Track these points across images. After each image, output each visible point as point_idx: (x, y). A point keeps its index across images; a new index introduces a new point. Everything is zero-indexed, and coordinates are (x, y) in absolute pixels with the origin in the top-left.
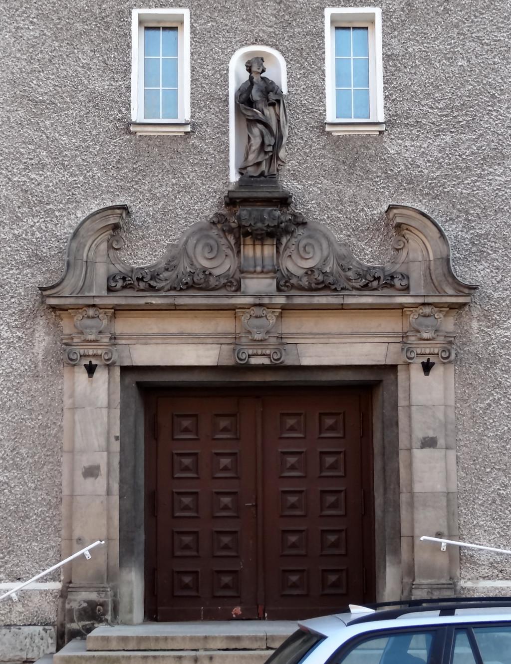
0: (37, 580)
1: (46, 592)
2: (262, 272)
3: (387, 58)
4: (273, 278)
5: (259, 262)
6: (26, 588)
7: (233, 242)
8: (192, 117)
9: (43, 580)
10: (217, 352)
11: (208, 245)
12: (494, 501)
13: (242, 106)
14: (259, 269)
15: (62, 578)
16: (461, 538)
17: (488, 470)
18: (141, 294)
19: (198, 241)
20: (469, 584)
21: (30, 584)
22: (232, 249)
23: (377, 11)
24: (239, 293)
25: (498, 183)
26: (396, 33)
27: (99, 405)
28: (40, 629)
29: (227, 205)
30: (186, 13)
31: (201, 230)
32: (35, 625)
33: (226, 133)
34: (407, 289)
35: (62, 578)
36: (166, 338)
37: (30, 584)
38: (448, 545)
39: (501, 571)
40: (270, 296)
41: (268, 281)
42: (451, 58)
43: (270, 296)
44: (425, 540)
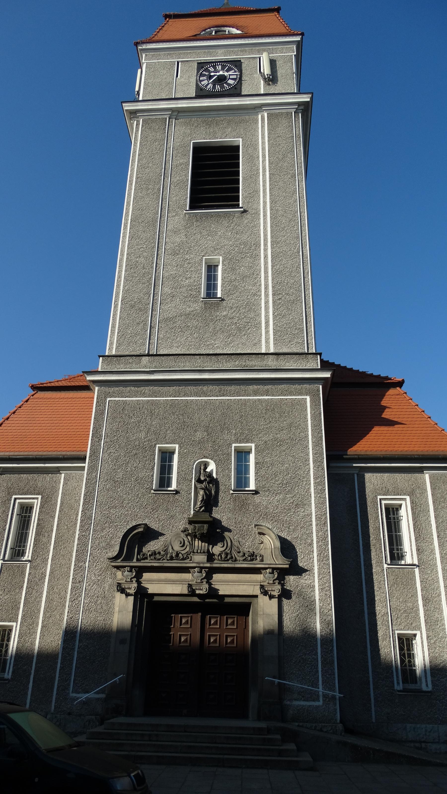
0: (95, 693)
1: (98, 699)
2: (201, 553)
3: (256, 464)
4: (205, 555)
5: (200, 548)
6: (89, 697)
7: (190, 540)
8: (177, 487)
9: (97, 693)
10: (181, 588)
11: (179, 540)
12: (300, 662)
13: (196, 483)
14: (199, 551)
15: (106, 692)
16: (284, 680)
17: (297, 646)
18: (151, 561)
19: (176, 539)
20: (288, 703)
21: (91, 695)
22: (189, 542)
23: (253, 445)
24: (191, 562)
25: (301, 515)
26: (260, 454)
27: (129, 611)
28: (93, 717)
29: (189, 524)
30: (177, 446)
31: (177, 534)
32: (92, 715)
33: (190, 494)
34: (262, 560)
35: (106, 692)
36: (159, 581)
37: (91, 695)
38: (279, 683)
39: (303, 697)
40: (203, 563)
41: (204, 556)
42: (283, 465)
43: (203, 563)
44: (267, 679)
